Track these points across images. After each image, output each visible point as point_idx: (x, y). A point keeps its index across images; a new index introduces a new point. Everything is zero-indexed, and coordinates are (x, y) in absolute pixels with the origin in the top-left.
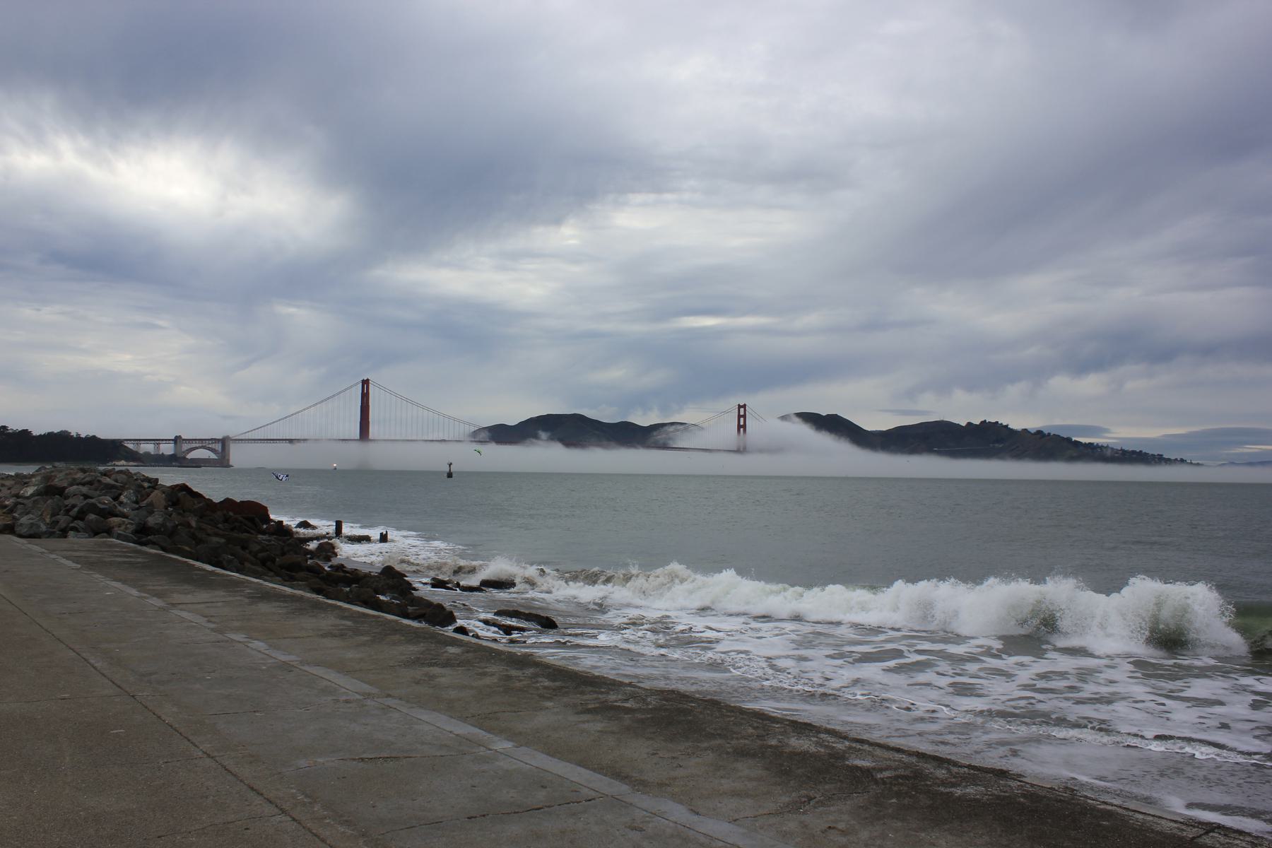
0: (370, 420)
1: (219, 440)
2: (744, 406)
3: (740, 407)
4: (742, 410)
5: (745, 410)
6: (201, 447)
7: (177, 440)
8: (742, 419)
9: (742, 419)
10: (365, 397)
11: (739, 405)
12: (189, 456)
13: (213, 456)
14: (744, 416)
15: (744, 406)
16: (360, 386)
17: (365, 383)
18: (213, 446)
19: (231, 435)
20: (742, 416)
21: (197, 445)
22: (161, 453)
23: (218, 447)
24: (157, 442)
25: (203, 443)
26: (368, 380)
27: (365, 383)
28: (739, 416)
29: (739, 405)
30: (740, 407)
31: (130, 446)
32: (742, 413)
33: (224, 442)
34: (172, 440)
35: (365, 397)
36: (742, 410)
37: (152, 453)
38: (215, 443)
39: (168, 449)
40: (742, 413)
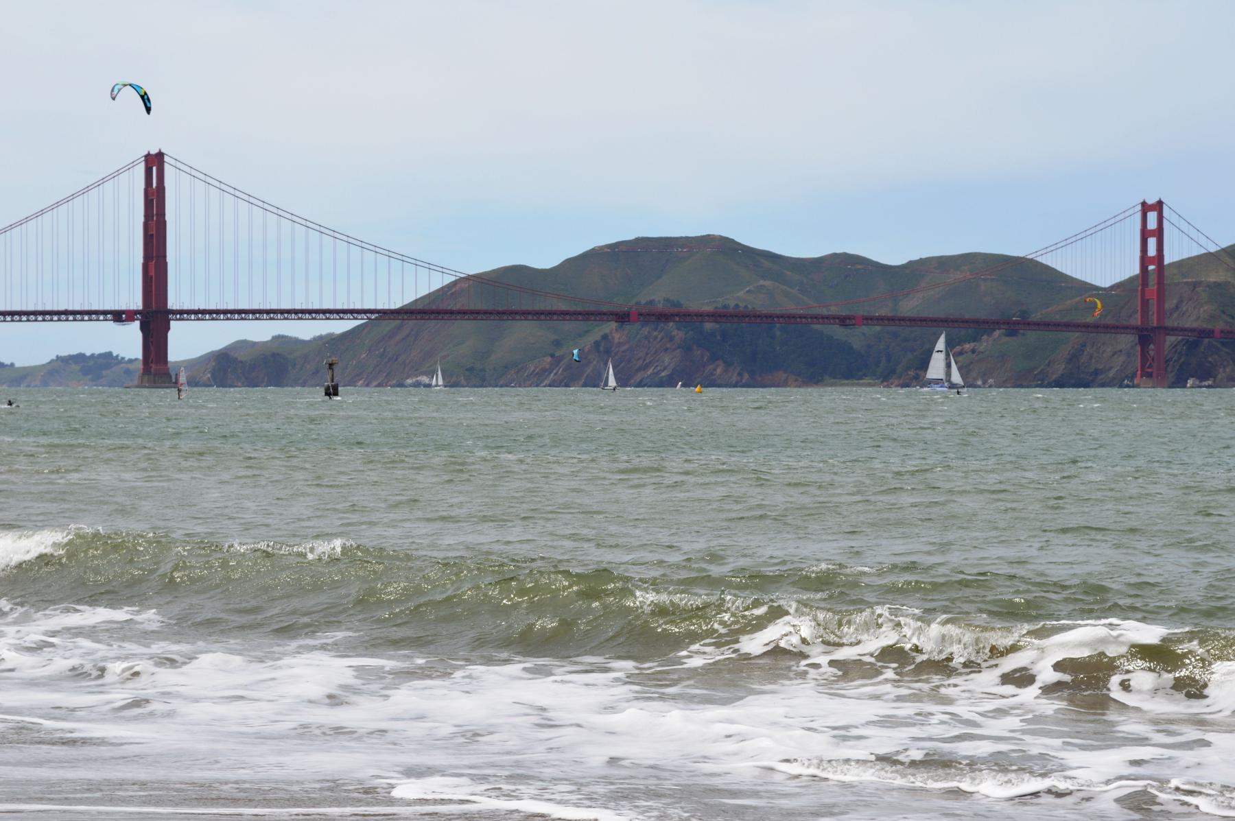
0: (169, 259)
2: (1159, 206)
3: (1145, 208)
4: (1152, 217)
8: (1152, 243)
9: (1152, 243)
11: (1144, 204)
14: (1159, 233)
15: (1159, 206)
20: (1152, 234)
26: (160, 155)
27: (155, 162)
28: (1145, 234)
29: (1144, 204)
30: (1145, 208)
32: (1152, 224)
36: (1152, 217)
40: (1152, 224)
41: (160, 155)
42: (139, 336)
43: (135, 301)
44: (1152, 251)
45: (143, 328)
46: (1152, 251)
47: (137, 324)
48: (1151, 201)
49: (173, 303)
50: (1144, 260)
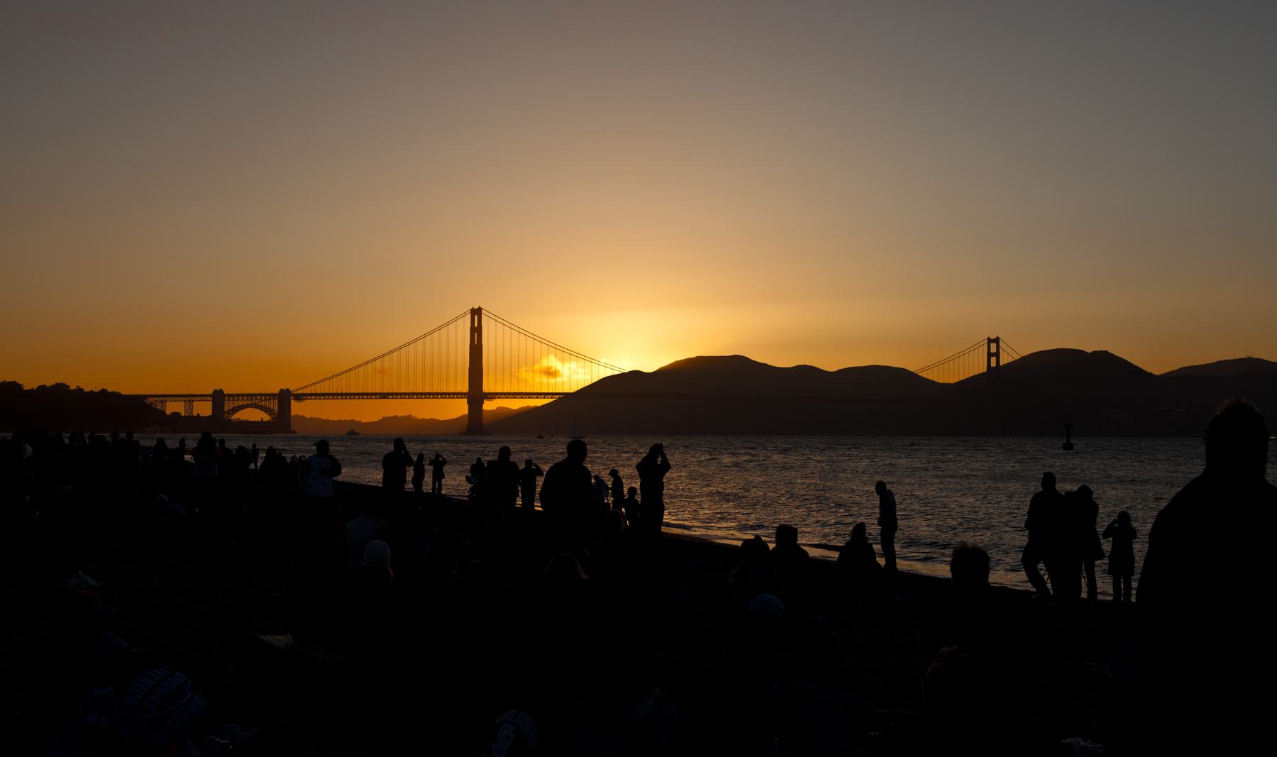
1: (274, 395)
2: (997, 340)
3: (990, 341)
4: (993, 346)
7: (218, 397)
8: (993, 360)
9: (993, 360)
10: (476, 331)
11: (989, 339)
13: (266, 417)
14: (997, 354)
16: (469, 317)
17: (476, 313)
18: (267, 404)
19: (291, 390)
20: (994, 355)
22: (195, 415)
23: (274, 405)
24: (189, 398)
25: (254, 400)
28: (990, 355)
29: (989, 339)
32: (993, 349)
33: (285, 397)
34: (210, 396)
35: (476, 331)
36: (993, 346)
37: (183, 415)
38: (270, 399)
40: (993, 349)
42: (466, 407)
43: (466, 389)
44: (993, 364)
45: (468, 402)
46: (993, 364)
47: (466, 400)
48: (993, 337)
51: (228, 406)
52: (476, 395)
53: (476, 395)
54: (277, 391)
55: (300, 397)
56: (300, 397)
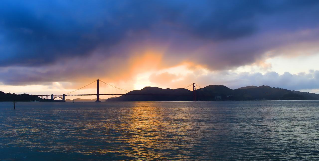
2: (195, 84)
3: (194, 84)
4: (194, 85)
5: (195, 85)
6: (58, 97)
7: (52, 95)
8: (194, 87)
9: (194, 87)
12: (55, 99)
13: (61, 99)
14: (195, 86)
15: (195, 84)
21: (57, 96)
23: (62, 97)
24: (47, 96)
25: (59, 96)
26: (99, 80)
27: (98, 80)
28: (194, 86)
30: (194, 84)
31: (41, 97)
32: (194, 86)
33: (64, 95)
36: (194, 85)
39: (50, 98)
40: (194, 86)
41: (99, 80)
46: (194, 88)
49: (100, 94)
50: (194, 89)
51: (54, 97)
52: (98, 95)
53: (98, 95)
54: (63, 95)
55: (66, 95)
56: (66, 95)
